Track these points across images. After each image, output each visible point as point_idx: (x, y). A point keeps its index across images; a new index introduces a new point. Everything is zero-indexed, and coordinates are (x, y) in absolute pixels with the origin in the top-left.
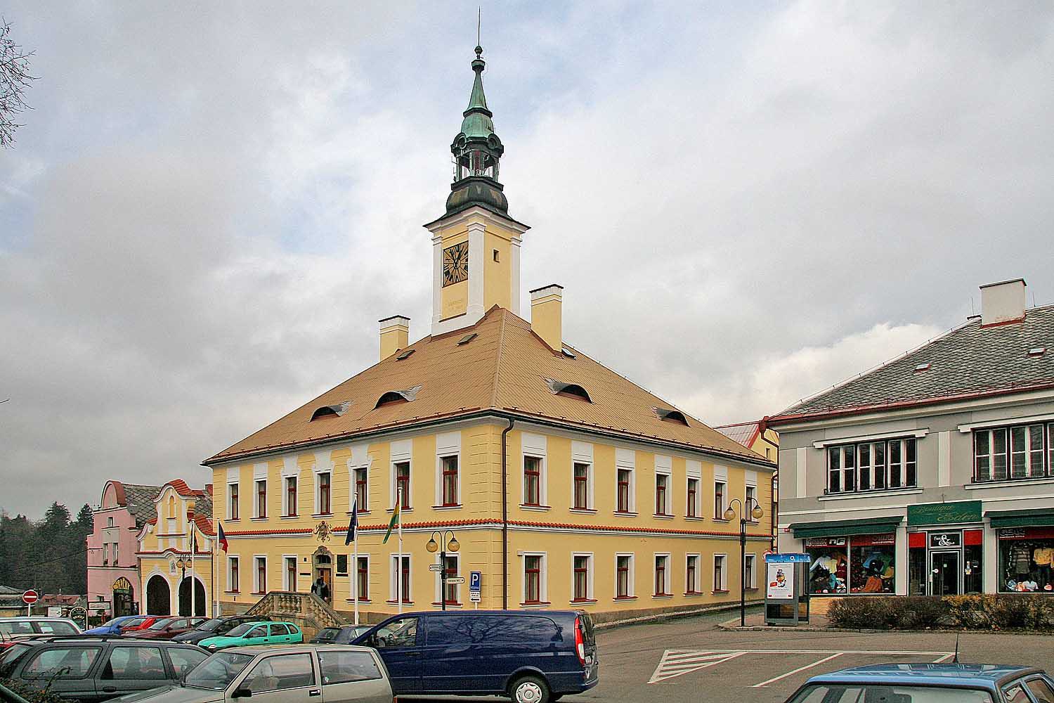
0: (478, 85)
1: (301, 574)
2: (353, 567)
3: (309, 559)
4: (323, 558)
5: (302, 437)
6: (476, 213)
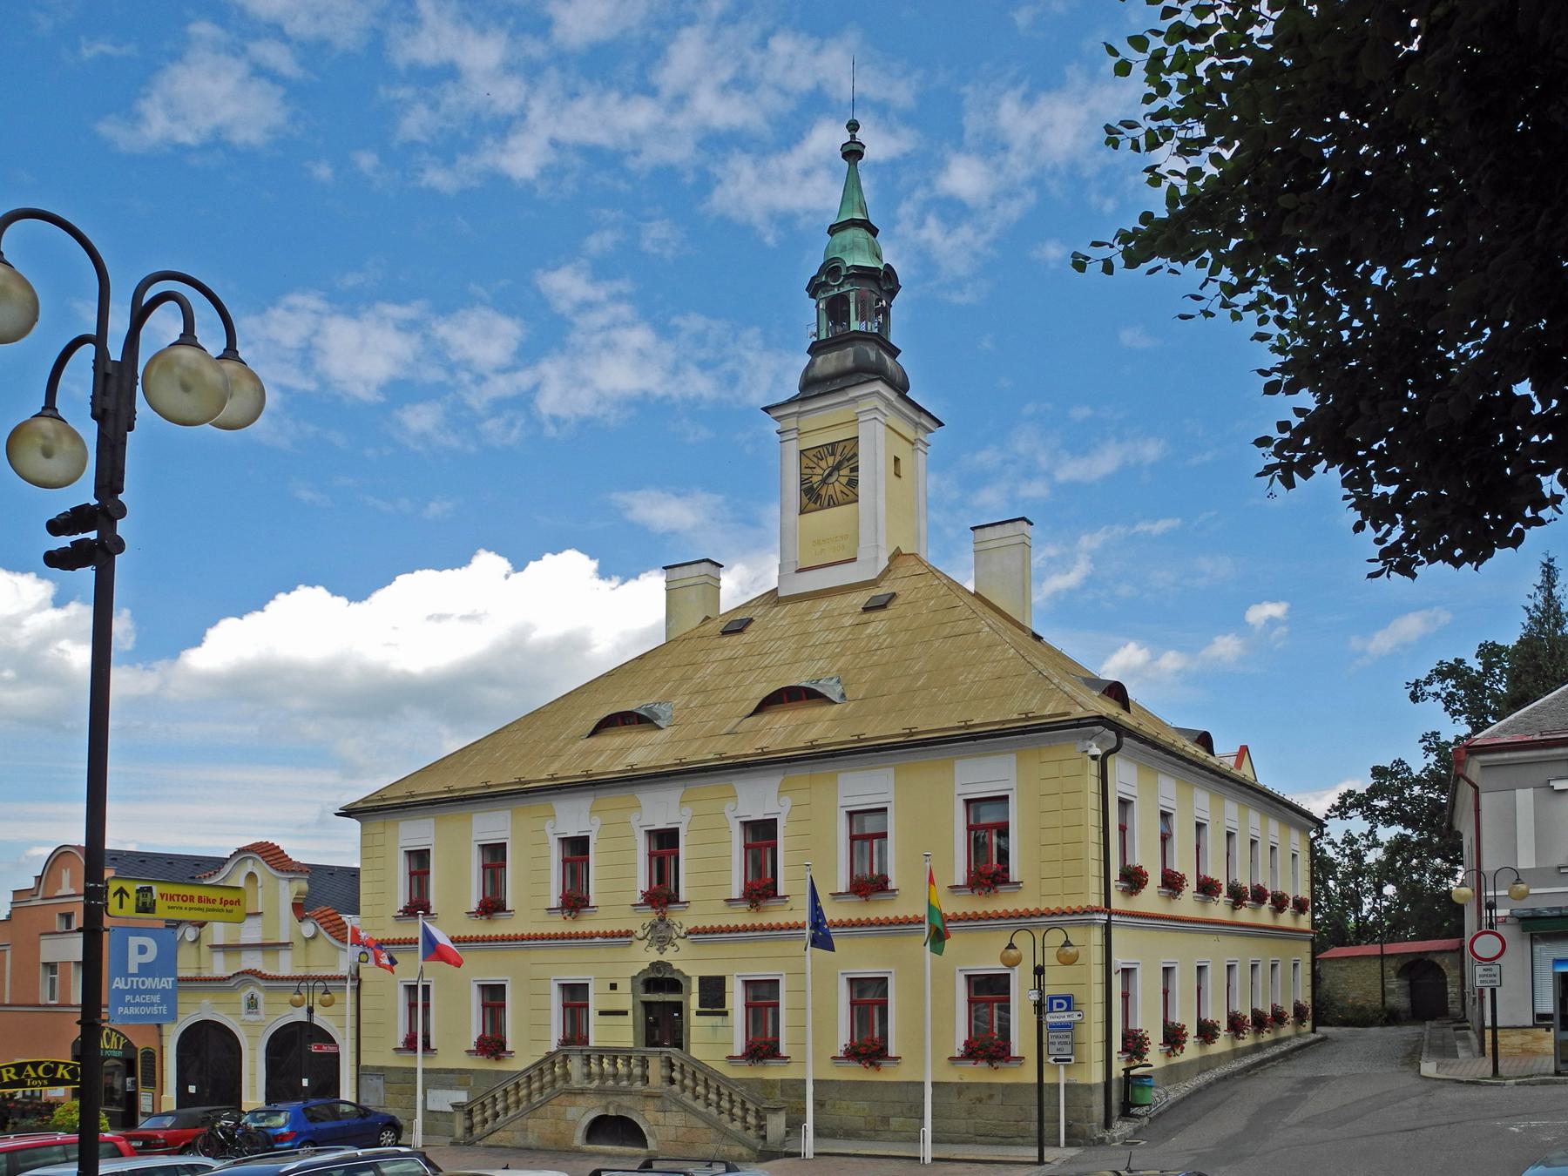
1: (602, 1013)
2: (736, 999)
3: (625, 986)
4: (660, 981)
5: (568, 766)
6: (878, 392)
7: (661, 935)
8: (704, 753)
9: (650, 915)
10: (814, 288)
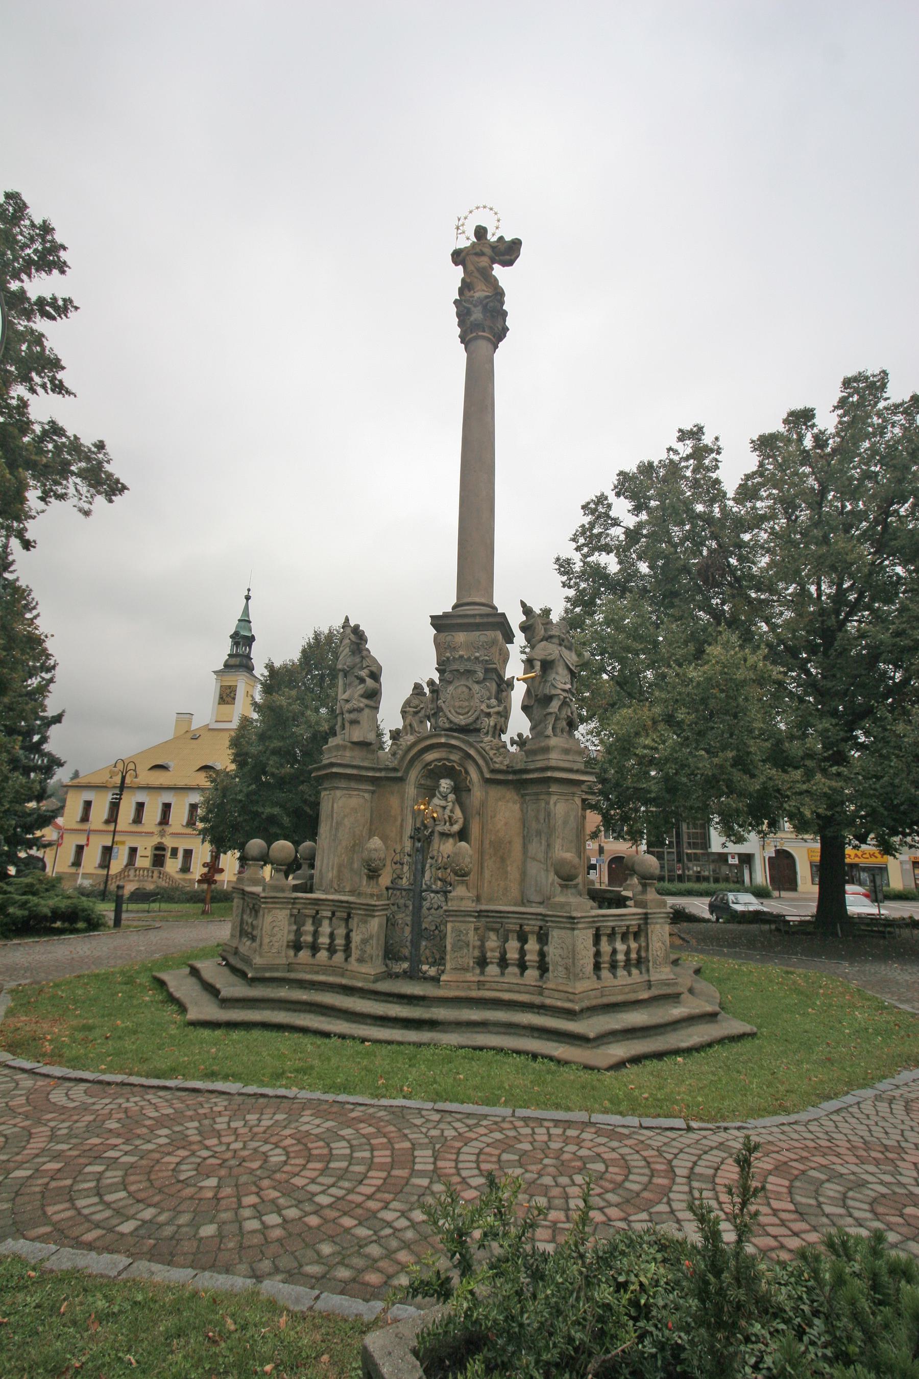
0: (247, 607)
3: (149, 849)
4: (160, 848)
7: (162, 834)
8: (181, 783)
9: (159, 828)
10: (231, 637)
